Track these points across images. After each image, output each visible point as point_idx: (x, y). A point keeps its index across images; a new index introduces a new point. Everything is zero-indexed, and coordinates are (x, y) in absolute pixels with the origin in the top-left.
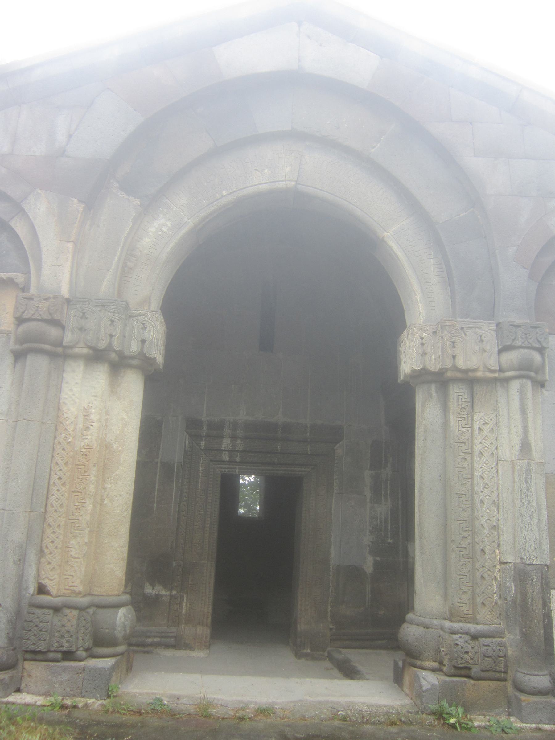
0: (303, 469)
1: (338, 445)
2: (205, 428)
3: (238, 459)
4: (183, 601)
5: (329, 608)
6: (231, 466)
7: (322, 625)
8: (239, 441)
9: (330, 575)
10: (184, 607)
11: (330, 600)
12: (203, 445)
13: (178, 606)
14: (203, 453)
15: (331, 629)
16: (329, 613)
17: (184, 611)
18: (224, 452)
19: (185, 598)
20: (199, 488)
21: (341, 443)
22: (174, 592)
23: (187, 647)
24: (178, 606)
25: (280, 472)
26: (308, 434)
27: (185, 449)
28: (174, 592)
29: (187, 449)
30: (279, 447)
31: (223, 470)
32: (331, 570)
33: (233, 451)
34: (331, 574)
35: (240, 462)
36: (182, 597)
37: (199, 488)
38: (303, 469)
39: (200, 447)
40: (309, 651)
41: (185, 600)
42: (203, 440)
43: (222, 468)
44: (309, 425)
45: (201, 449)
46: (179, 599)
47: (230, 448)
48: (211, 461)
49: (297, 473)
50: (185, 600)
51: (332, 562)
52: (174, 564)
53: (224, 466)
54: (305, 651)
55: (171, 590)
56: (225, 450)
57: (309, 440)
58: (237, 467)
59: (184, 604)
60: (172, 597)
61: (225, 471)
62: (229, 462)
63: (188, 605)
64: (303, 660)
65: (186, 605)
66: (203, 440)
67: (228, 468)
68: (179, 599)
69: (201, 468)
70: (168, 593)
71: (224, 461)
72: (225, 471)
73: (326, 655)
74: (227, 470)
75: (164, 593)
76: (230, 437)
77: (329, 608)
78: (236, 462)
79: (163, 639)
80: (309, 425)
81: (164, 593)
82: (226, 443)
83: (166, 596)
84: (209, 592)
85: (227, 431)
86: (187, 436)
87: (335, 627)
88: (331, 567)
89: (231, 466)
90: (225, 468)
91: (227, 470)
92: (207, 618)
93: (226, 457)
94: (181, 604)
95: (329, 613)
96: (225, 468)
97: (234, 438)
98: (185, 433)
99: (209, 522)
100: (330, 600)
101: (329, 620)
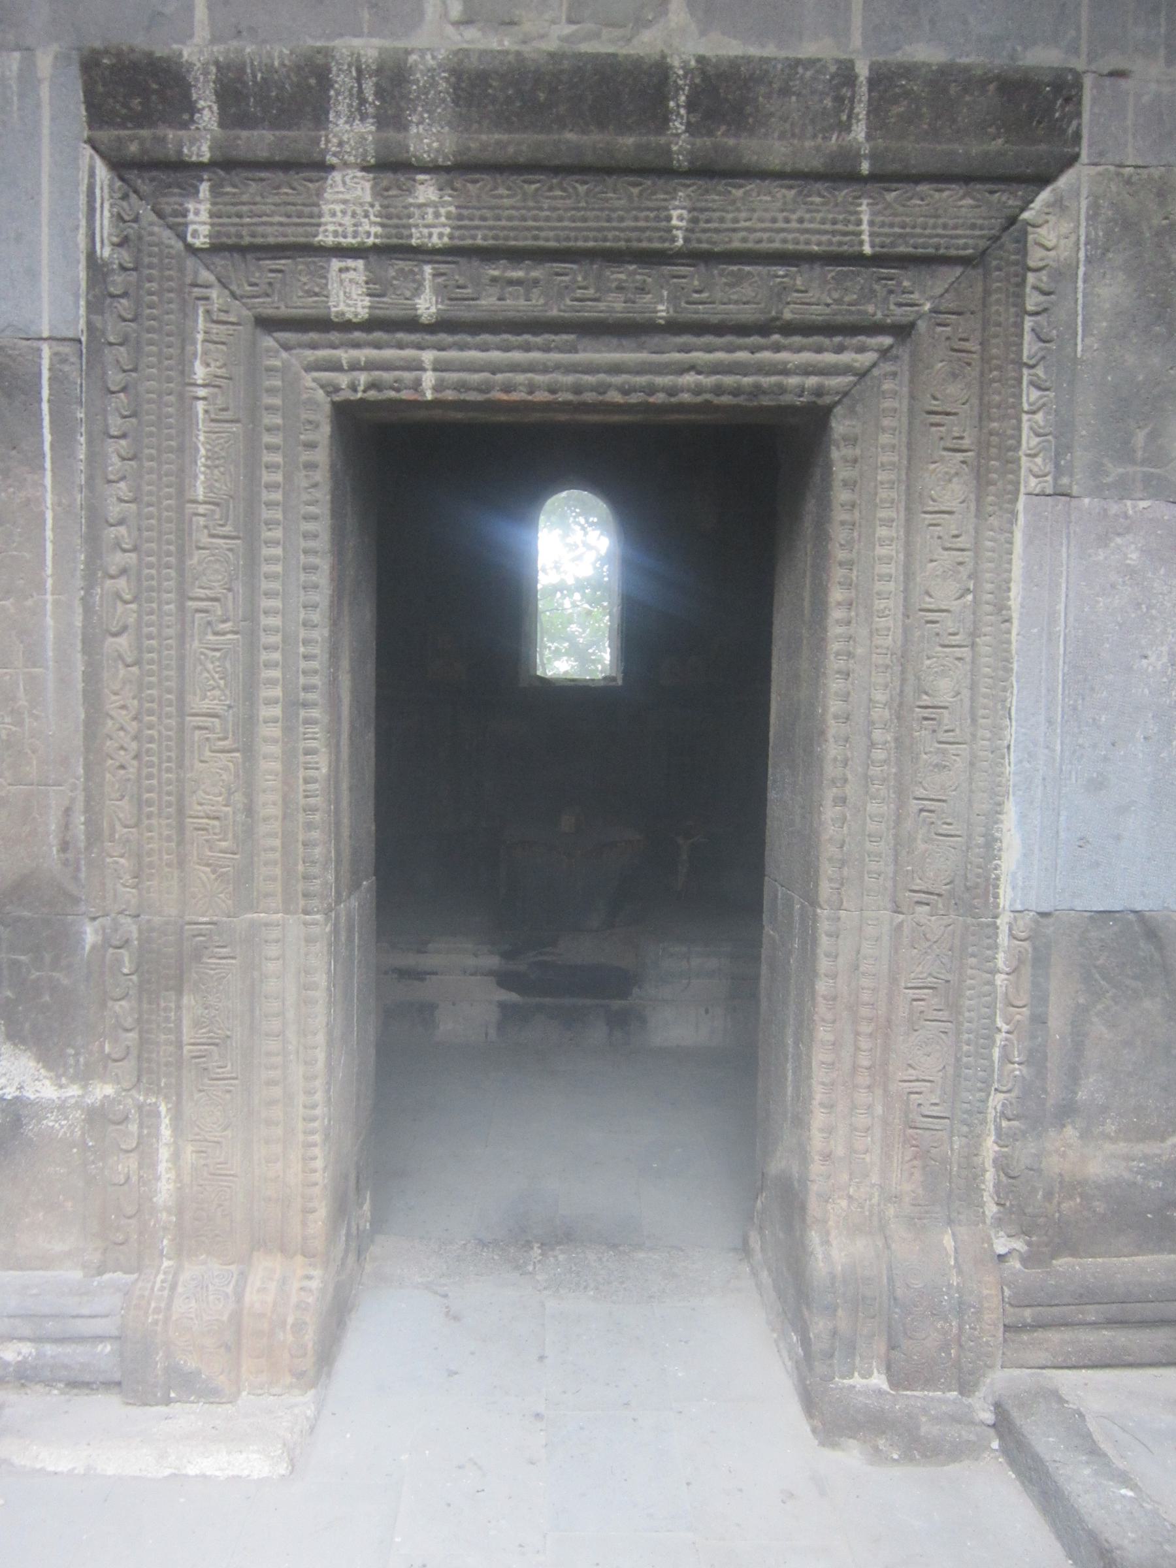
0: (829, 358)
1: (1045, 195)
2: (208, 116)
3: (427, 306)
4: (157, 1135)
5: (990, 1147)
6: (389, 354)
7: (948, 1241)
8: (426, 191)
9: (994, 971)
10: (162, 1167)
11: (996, 1101)
12: (200, 219)
13: (132, 1162)
14: (206, 276)
15: (1001, 1258)
16: (990, 1175)
17: (165, 1190)
18: (336, 264)
19: (166, 1121)
20: (200, 492)
21: (1064, 182)
22: (103, 1090)
23: (183, 1385)
24: (132, 1162)
25: (690, 379)
26: (859, 132)
27: (91, 255)
28: (103, 1090)
29: (105, 252)
30: (678, 218)
31: (343, 380)
32: (1003, 939)
33: (394, 251)
34: (1001, 960)
35: (443, 325)
36: (148, 1115)
37: (200, 492)
38: (829, 358)
39: (182, 237)
40: (879, 1381)
41: (166, 1132)
42: (204, 188)
43: (337, 367)
44: (863, 71)
45: (190, 248)
46: (133, 1128)
47: (371, 232)
48: (267, 324)
49: (793, 381)
50: (166, 1132)
51: (1006, 897)
52: (90, 935)
53: (345, 355)
54: (857, 1381)
55: (84, 1077)
56: (341, 251)
57: (865, 167)
58: (428, 356)
59: (164, 1154)
60: (97, 1117)
61: (353, 388)
62: (371, 324)
63: (189, 1154)
64: (850, 1457)
65: (176, 1157)
66: (204, 188)
67: (370, 366)
68: (133, 1128)
69: (200, 372)
70: (74, 1091)
71: (347, 326)
72: (353, 388)
73: (988, 1416)
74: (363, 378)
75: (44, 1089)
76: (365, 169)
77: (990, 1147)
78: (412, 324)
79: (49, 1349)
80: (863, 71)
81: (44, 1089)
82: (347, 206)
83: (62, 1108)
84: (309, 1078)
85: (348, 132)
86: (102, 172)
87: (1019, 1245)
88: (1003, 922)
89: (389, 354)
90: (354, 367)
91: (363, 378)
92: (306, 1211)
93: (348, 293)
94: (144, 1150)
95: (990, 1175)
96: (354, 367)
97: (392, 167)
98: (88, 151)
99: (277, 692)
100: (996, 1101)
101: (991, 1209)
